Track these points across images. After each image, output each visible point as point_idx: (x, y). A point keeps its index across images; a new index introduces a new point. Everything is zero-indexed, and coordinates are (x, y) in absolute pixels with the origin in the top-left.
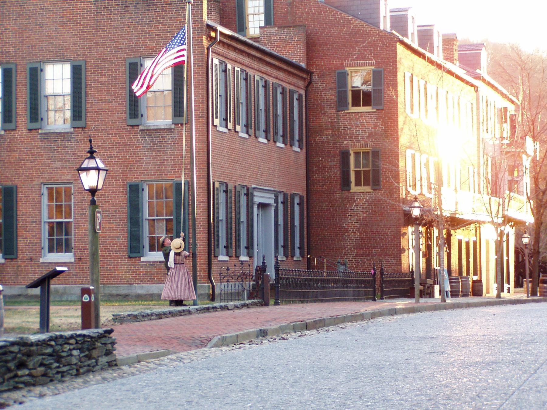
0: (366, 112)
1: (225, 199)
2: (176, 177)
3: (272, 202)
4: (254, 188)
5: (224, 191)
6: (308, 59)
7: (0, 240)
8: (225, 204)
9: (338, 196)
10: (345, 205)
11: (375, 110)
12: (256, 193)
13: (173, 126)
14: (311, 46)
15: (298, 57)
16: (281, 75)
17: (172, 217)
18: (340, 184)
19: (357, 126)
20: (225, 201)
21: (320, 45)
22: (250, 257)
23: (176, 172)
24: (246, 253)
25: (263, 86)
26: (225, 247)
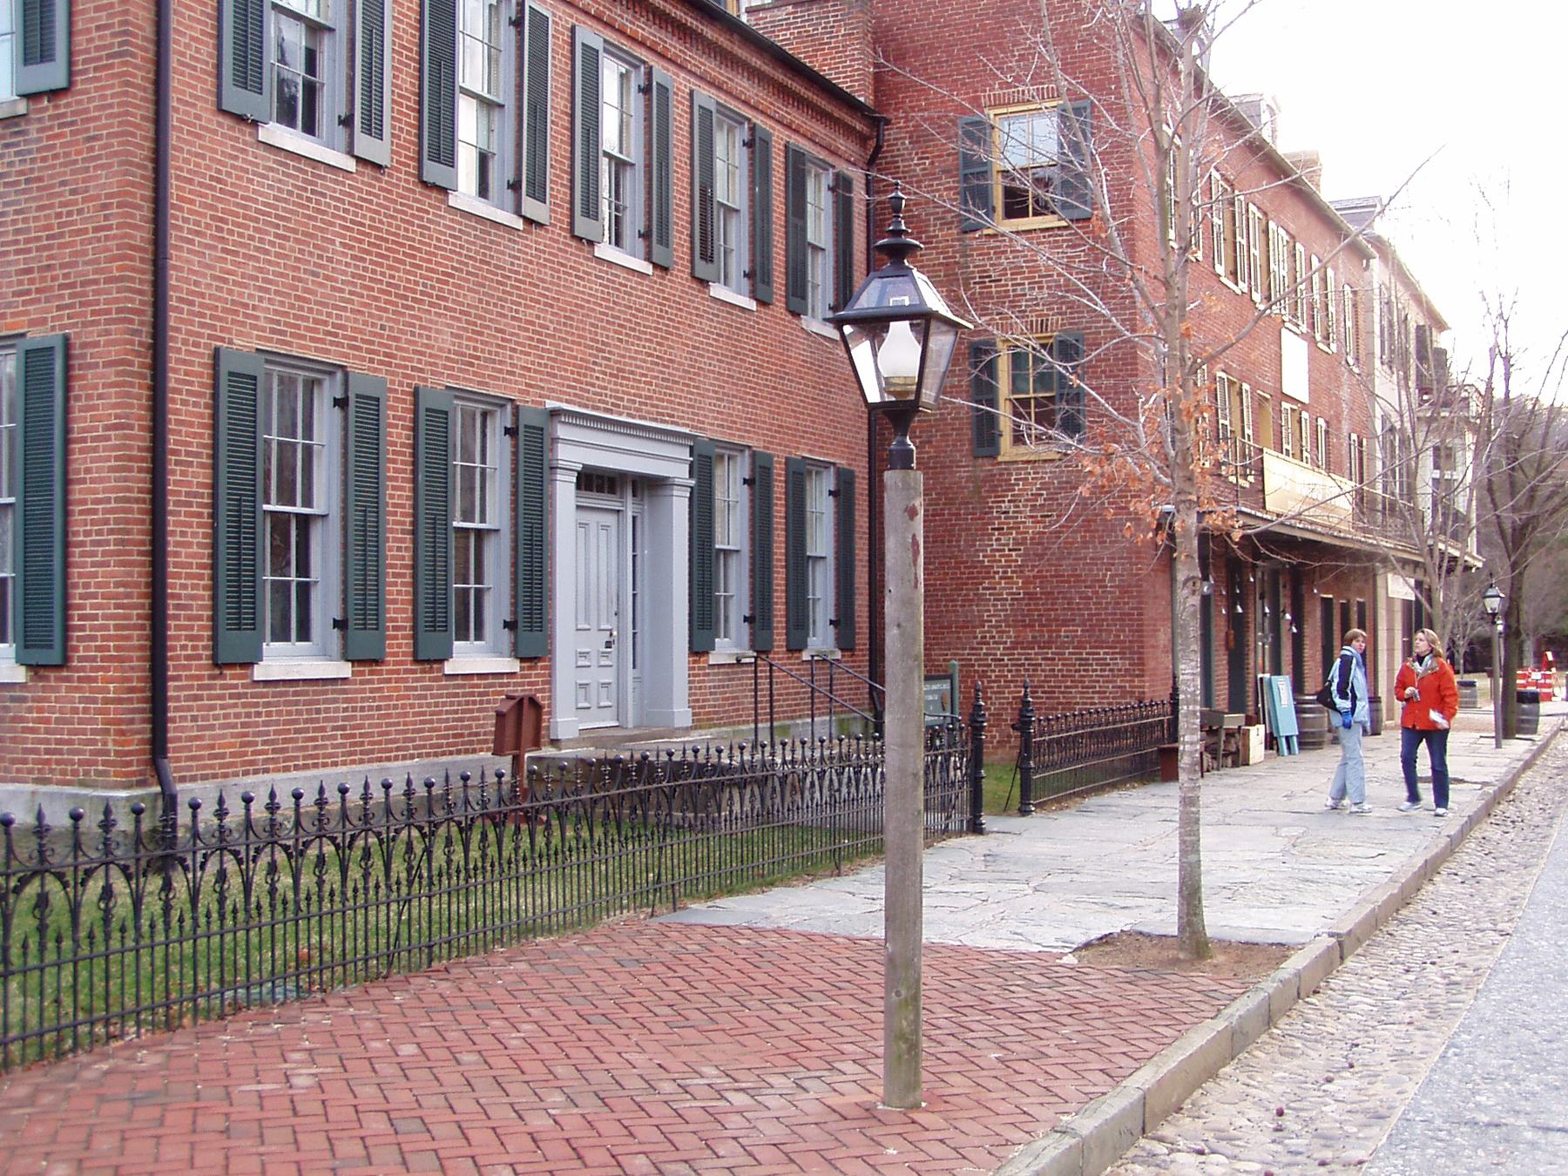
0: (1043, 230)
1: (508, 456)
2: (32, 323)
3: (678, 471)
4: (555, 413)
5: (507, 431)
6: (876, 91)
7: (4, 580)
8: (508, 474)
9: (963, 473)
10: (984, 501)
11: (1064, 224)
12: (562, 431)
13: (22, 108)
14: (886, 43)
15: (849, 71)
16: (742, 84)
17: (12, 500)
18: (971, 441)
19: (1017, 271)
20: (508, 466)
21: (916, 55)
22: (528, 660)
23: (32, 302)
24: (507, 647)
25: (640, 89)
26: (336, 624)
